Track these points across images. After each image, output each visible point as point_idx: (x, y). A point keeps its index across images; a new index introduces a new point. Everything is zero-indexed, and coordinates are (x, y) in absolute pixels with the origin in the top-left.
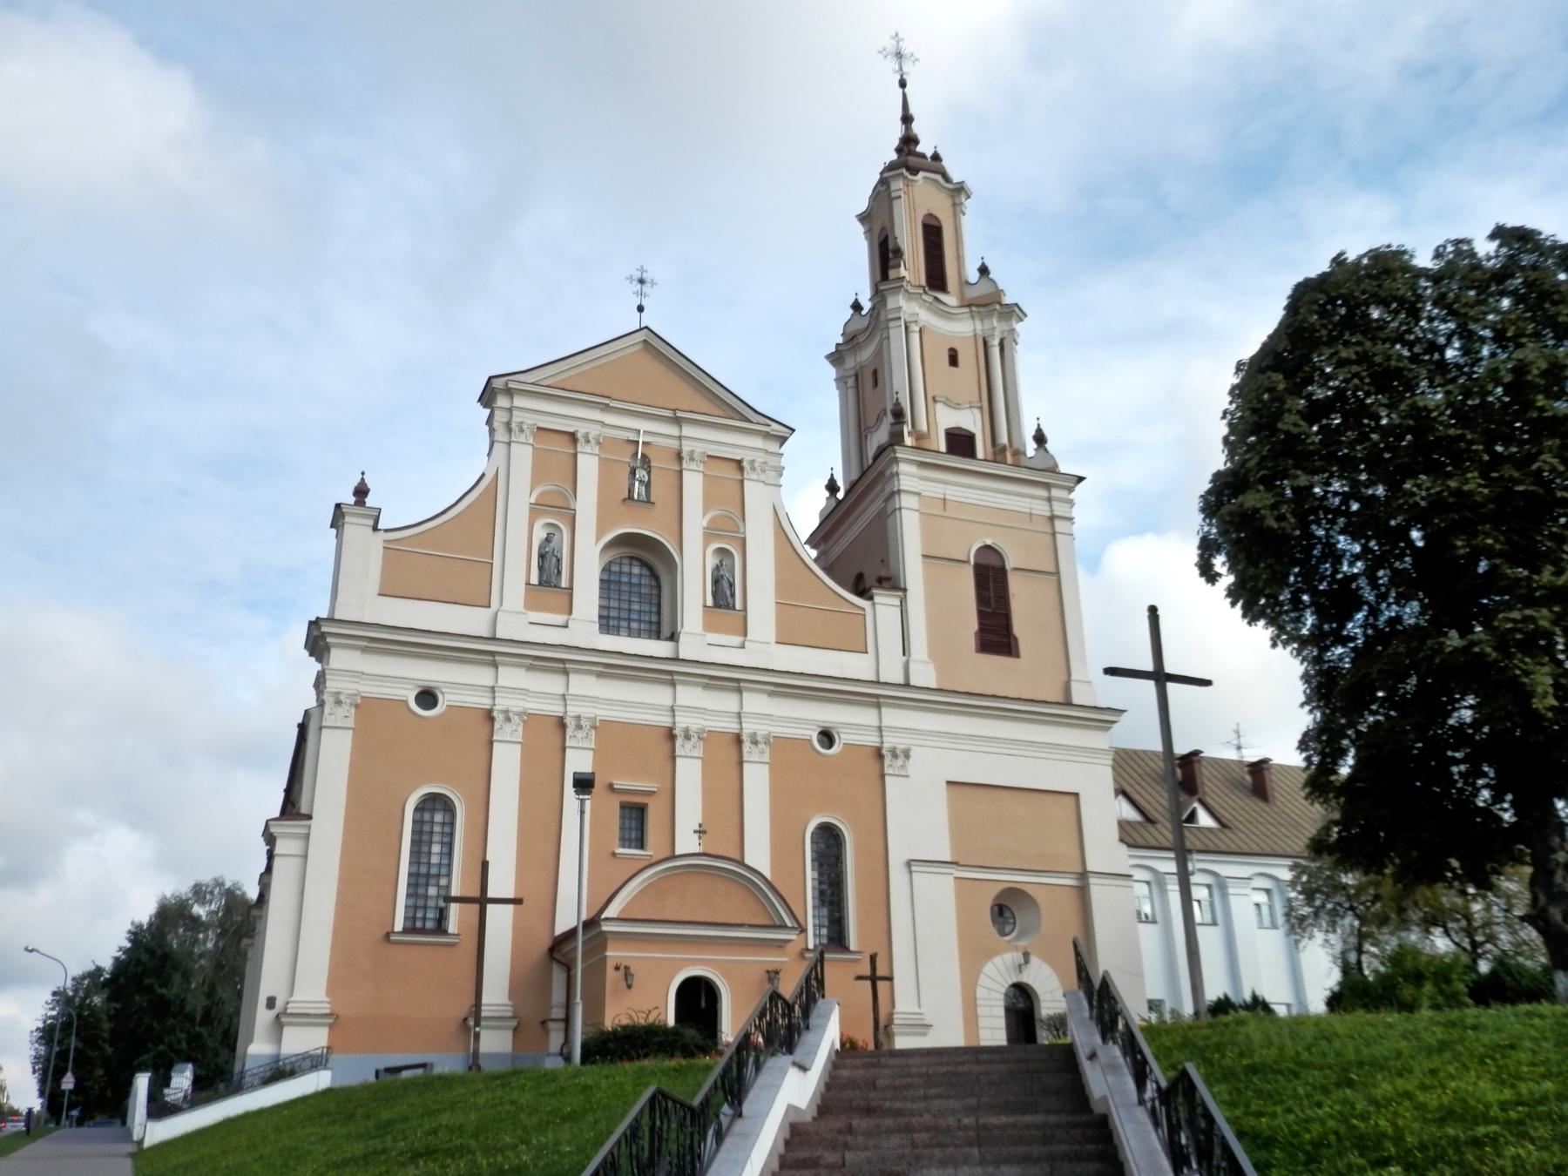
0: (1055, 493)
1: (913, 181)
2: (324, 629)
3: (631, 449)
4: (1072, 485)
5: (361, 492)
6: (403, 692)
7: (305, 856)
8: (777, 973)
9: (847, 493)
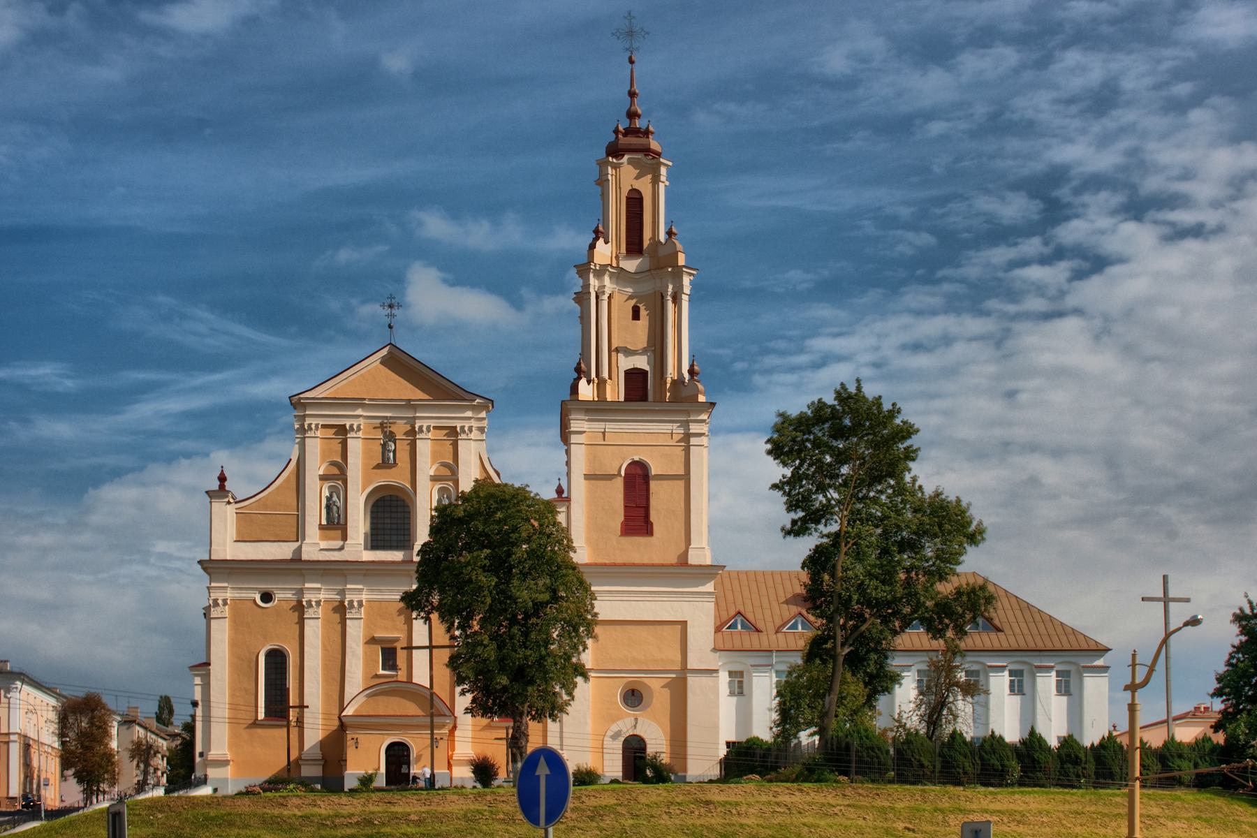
5: (222, 479)
6: (253, 595)
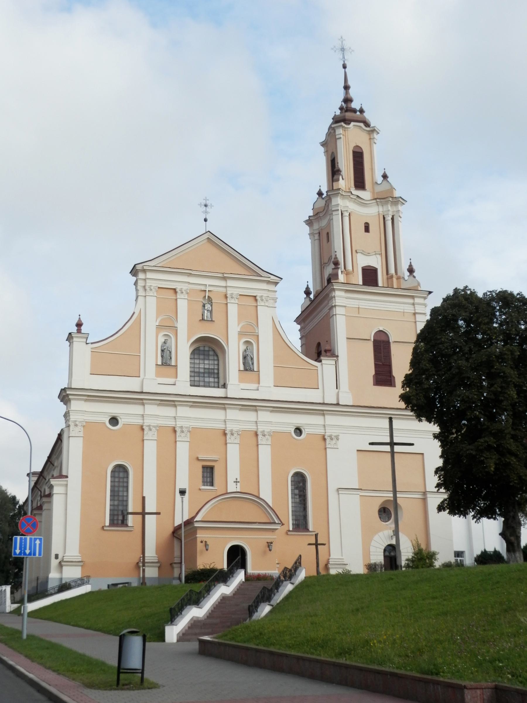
0: (417, 300)
1: (347, 128)
2: (68, 392)
3: (203, 294)
4: (426, 296)
5: (79, 325)
6: (104, 419)
7: (67, 494)
8: (272, 543)
9: (316, 297)
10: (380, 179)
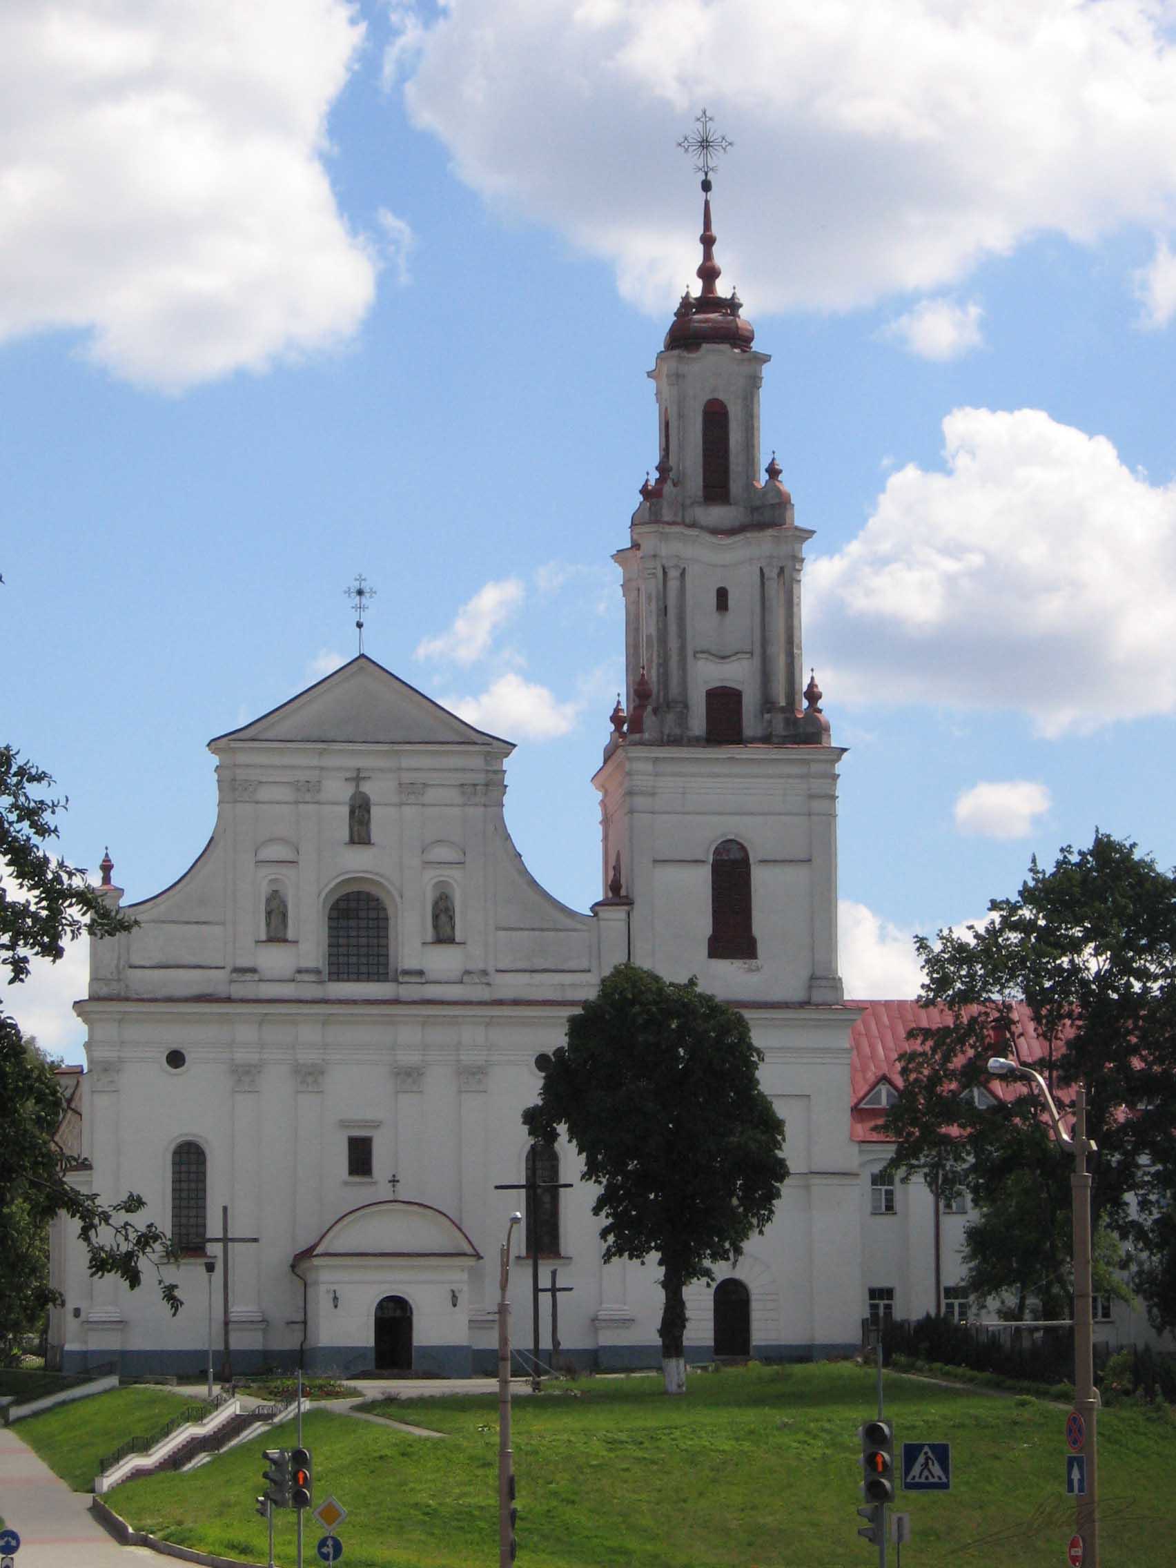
0: (815, 768)
10: (764, 477)
